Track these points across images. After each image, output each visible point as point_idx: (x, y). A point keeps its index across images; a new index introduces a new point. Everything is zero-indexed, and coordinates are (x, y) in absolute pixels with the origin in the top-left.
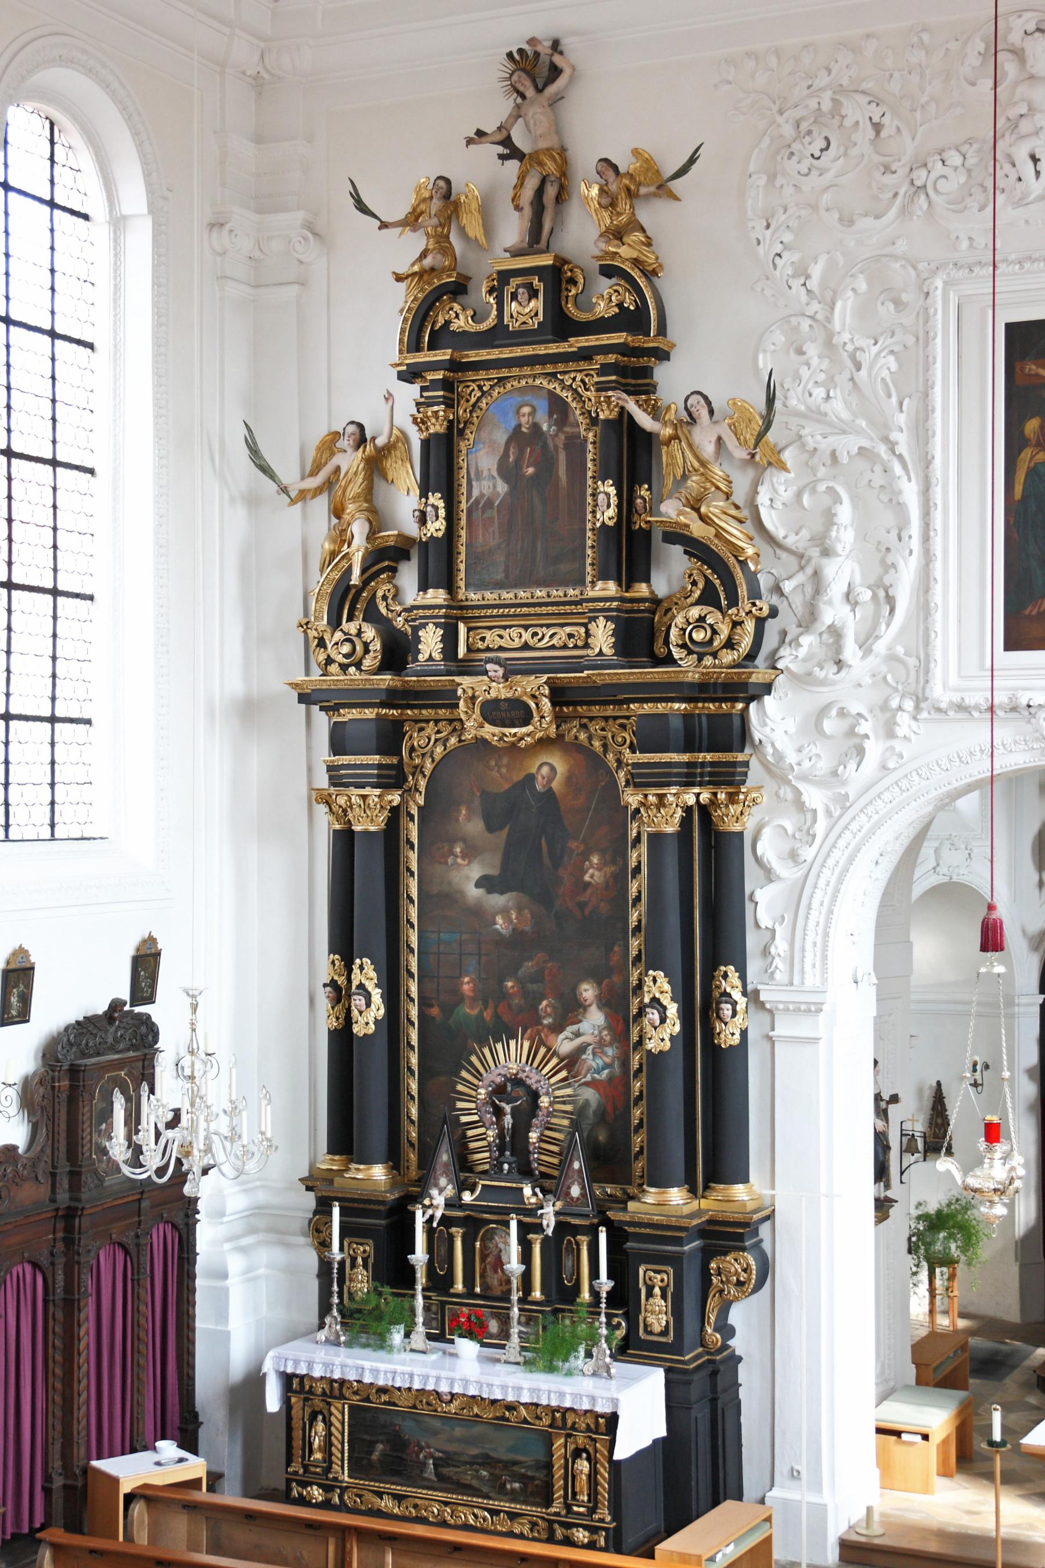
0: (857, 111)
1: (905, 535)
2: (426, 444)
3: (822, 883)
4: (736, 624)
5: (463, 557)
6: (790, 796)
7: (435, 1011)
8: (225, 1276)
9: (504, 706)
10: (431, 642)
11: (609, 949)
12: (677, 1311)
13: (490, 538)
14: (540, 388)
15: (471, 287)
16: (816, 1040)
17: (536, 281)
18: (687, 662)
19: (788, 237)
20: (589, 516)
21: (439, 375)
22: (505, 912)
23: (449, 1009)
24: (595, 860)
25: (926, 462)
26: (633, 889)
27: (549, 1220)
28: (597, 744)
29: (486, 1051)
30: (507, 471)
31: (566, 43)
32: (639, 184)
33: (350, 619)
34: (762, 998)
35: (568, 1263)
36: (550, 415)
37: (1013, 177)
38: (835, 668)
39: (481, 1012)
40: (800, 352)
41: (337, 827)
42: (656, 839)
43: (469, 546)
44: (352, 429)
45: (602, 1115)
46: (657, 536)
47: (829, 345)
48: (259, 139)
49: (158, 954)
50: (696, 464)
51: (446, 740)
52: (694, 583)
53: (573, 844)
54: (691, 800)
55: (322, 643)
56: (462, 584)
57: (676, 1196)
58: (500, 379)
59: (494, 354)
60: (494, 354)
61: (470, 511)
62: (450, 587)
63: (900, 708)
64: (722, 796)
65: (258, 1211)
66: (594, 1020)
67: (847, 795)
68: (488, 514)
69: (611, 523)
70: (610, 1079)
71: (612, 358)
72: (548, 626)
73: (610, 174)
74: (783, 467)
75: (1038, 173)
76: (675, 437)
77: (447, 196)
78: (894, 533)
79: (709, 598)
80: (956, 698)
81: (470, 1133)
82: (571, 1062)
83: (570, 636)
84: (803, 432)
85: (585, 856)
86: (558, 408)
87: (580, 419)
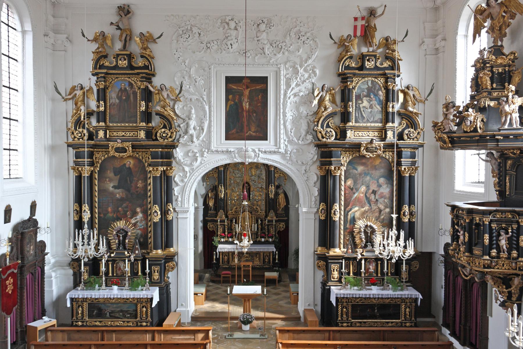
0: (195, 30)
1: (205, 116)
2: (98, 91)
3: (188, 186)
5: (108, 116)
6: (181, 168)
7: (102, 215)
9: (120, 149)
10: (101, 134)
11: (143, 201)
12: (160, 275)
14: (126, 80)
15: (108, 56)
17: (125, 57)
18: (161, 140)
19: (181, 54)
21: (103, 75)
22: (119, 193)
23: (105, 215)
24: (140, 182)
25: (210, 102)
26: (149, 188)
27: (132, 258)
28: (141, 157)
29: (115, 223)
30: (119, 97)
31: (131, 6)
32: (149, 39)
33: (79, 128)
34: (176, 210)
36: (129, 86)
37: (227, 47)
40: (184, 78)
41: (76, 175)
42: (155, 178)
43: (109, 113)
44: (79, 85)
45: (141, 235)
46: (154, 114)
47: (190, 76)
48: (54, 17)
49: (36, 205)
50: (163, 99)
51: (104, 156)
52: (161, 124)
53: (135, 179)
54: (162, 169)
55: (73, 133)
56: (108, 121)
57: (160, 251)
58: (117, 77)
59: (114, 72)
60: (114, 72)
62: (105, 122)
63: (205, 151)
64: (169, 168)
65: (56, 262)
66: (140, 216)
68: (114, 107)
70: (144, 228)
71: (144, 75)
72: (129, 132)
73: (143, 36)
74: (180, 101)
75: (232, 48)
76: (158, 93)
77: (104, 36)
78: (203, 116)
79: (165, 127)
80: (216, 149)
81: (111, 241)
82: (135, 225)
83: (134, 134)
84: (184, 94)
85: (138, 181)
86: (131, 85)
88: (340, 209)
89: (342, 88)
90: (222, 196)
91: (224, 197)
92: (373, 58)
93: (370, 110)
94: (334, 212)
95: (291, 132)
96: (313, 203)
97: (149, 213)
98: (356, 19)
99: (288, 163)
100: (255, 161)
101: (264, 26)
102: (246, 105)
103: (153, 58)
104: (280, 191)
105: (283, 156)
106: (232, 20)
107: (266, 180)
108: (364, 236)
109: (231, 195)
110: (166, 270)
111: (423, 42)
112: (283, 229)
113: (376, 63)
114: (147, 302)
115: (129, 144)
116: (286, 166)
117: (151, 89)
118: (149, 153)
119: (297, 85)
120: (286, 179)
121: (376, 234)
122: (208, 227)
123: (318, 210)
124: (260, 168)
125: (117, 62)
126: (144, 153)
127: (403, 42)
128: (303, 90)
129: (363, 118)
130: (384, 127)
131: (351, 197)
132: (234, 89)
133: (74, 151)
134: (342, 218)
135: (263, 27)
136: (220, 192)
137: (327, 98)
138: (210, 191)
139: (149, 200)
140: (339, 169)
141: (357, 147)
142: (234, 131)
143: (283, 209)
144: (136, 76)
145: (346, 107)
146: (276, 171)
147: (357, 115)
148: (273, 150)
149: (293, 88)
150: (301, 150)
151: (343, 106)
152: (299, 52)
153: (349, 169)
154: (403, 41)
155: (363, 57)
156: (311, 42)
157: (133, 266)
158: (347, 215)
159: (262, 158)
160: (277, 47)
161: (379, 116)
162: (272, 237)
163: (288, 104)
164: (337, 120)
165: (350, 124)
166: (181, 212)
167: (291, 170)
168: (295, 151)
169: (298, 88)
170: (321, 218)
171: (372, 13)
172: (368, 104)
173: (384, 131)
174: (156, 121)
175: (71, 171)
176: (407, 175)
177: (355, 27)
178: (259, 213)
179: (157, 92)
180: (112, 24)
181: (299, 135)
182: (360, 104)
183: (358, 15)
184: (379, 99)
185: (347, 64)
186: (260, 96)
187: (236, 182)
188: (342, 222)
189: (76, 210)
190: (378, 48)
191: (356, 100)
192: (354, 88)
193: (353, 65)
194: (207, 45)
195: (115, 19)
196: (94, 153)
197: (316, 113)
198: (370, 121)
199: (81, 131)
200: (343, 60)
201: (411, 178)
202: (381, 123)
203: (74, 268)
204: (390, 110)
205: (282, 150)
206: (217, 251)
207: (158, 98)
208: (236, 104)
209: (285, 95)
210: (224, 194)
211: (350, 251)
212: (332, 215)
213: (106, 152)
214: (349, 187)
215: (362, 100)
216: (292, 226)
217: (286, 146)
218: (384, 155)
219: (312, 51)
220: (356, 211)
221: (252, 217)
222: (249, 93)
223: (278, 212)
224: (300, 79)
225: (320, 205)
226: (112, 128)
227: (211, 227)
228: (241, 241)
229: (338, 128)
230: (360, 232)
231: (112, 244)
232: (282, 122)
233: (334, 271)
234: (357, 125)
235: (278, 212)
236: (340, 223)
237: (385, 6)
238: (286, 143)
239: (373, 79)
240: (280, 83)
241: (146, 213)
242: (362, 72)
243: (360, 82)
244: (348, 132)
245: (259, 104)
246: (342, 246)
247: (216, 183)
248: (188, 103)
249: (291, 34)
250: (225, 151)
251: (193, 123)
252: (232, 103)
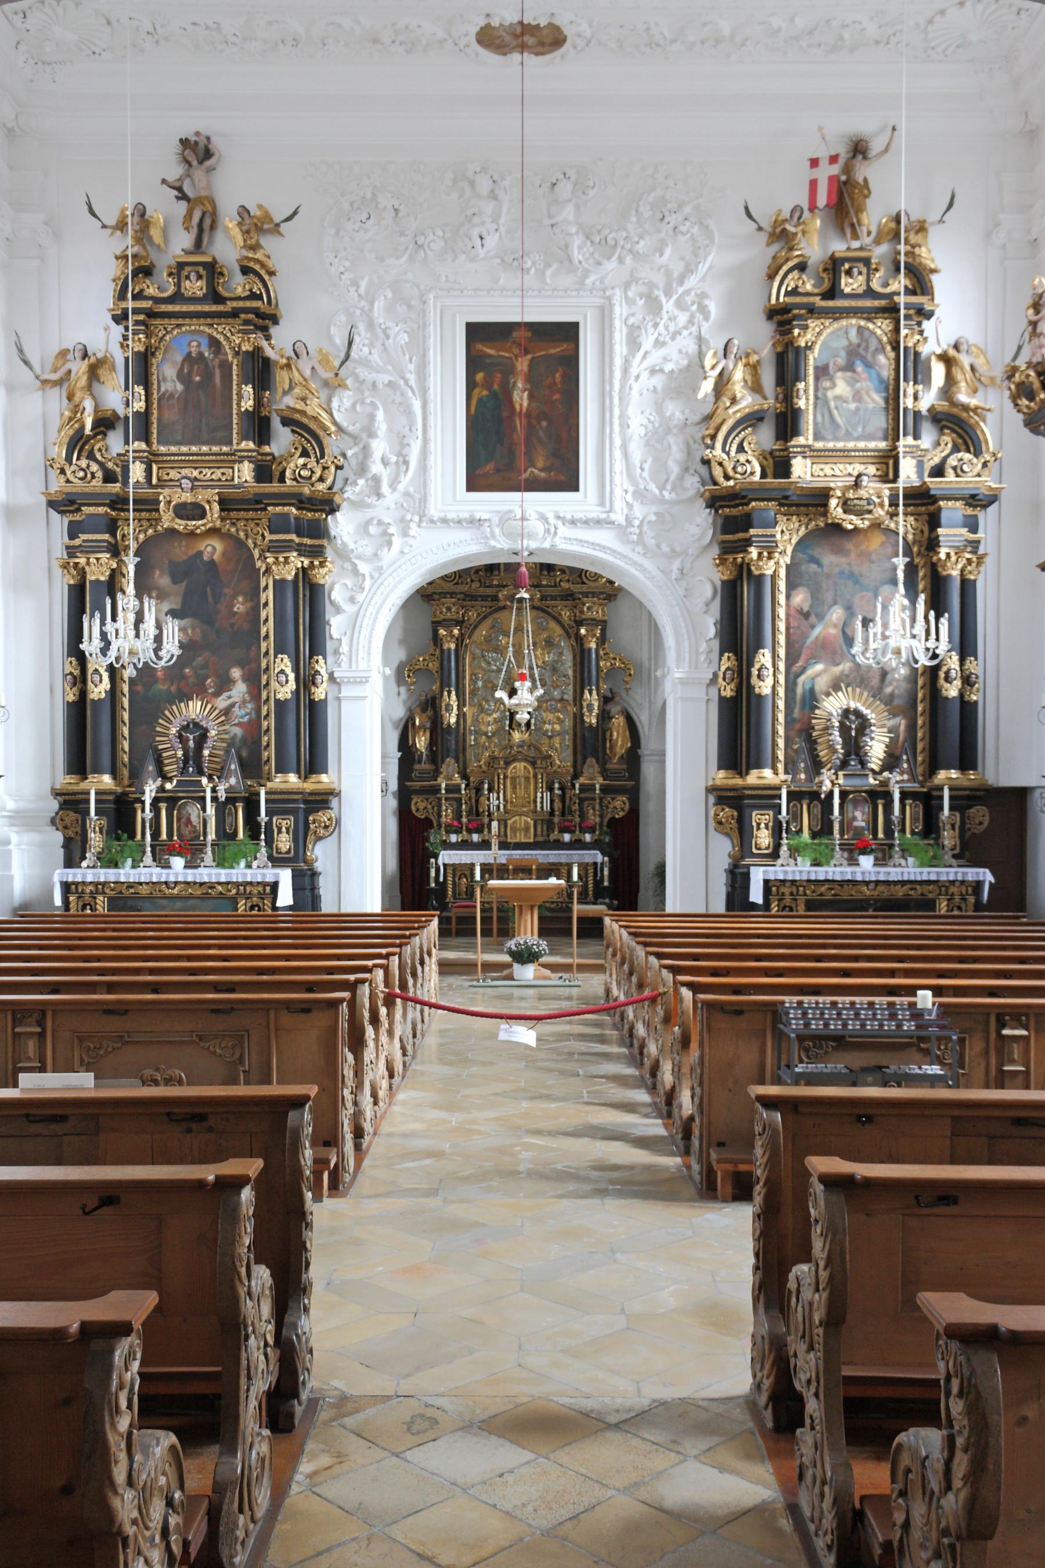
1: (414, 429)
3: (368, 614)
4: (324, 468)
5: (155, 425)
6: (350, 567)
7: (139, 688)
8: (8, 842)
9: (189, 507)
11: (249, 648)
12: (295, 840)
13: (171, 416)
14: (203, 332)
15: (155, 272)
16: (364, 698)
17: (201, 269)
20: (235, 406)
24: (240, 599)
25: (424, 391)
26: (263, 615)
28: (242, 535)
29: (174, 708)
30: (181, 377)
31: (212, 139)
32: (263, 223)
34: (336, 675)
35: (229, 820)
36: (210, 346)
37: (470, 246)
38: (376, 498)
39: (169, 688)
41: (72, 582)
42: (279, 585)
43: (159, 419)
45: (244, 740)
46: (276, 422)
47: (371, 325)
50: (301, 379)
51: (145, 531)
52: (296, 449)
53: (226, 591)
54: (299, 565)
55: (63, 471)
56: (155, 441)
61: (159, 400)
62: (148, 443)
63: (411, 520)
64: (316, 563)
66: (240, 690)
67: (382, 567)
68: (171, 402)
69: (251, 409)
70: (250, 721)
71: (251, 316)
72: (209, 468)
73: (246, 216)
76: (288, 366)
77: (143, 215)
78: (407, 428)
79: (305, 454)
80: (442, 515)
81: (164, 755)
82: (227, 712)
84: (357, 371)
85: (234, 597)
86: (214, 343)
87: (229, 351)
88: (774, 665)
89: (779, 349)
90: (453, 720)
91: (458, 722)
92: (861, 265)
93: (853, 406)
94: (759, 670)
95: (642, 469)
96: (703, 657)
97: (264, 682)
98: (814, 163)
99: (633, 550)
100: (547, 545)
101: (569, 187)
102: (521, 399)
103: (271, 273)
104: (614, 709)
105: (622, 531)
106: (484, 170)
107: (575, 677)
108: (840, 740)
109: (476, 721)
110: (310, 833)
111: (997, 224)
112: (622, 814)
113: (868, 280)
114: (261, 896)
115: (212, 494)
116: (630, 559)
117: (269, 353)
118: (265, 522)
119: (659, 344)
120: (630, 675)
121: (872, 732)
122: (413, 808)
123: (715, 675)
124: (558, 646)
125: (178, 285)
126: (252, 524)
127: (942, 225)
128: (675, 356)
129: (837, 426)
130: (891, 451)
131: (805, 637)
132: (490, 356)
133: (66, 521)
134: (781, 692)
135: (565, 189)
136: (447, 710)
137: (739, 374)
138: (418, 710)
139: (264, 645)
140: (770, 558)
141: (819, 499)
142: (489, 467)
143: (622, 757)
144: (230, 320)
145: (788, 396)
146: (601, 653)
147: (819, 419)
148: (594, 515)
149: (646, 353)
150: (668, 517)
151: (781, 397)
152: (661, 255)
153: (797, 561)
154: (941, 221)
155: (834, 266)
156: (695, 230)
157: (223, 808)
158: (795, 684)
159: (565, 538)
160: (603, 242)
161: (880, 422)
162: (592, 830)
163: (635, 393)
164: (765, 437)
165: (801, 440)
166: (349, 682)
167: (643, 570)
168: (653, 518)
169: (662, 352)
170: (723, 694)
171: (859, 149)
172: (848, 389)
173: (891, 462)
174: (282, 440)
175: (58, 572)
176: (955, 573)
177: (813, 184)
178: (555, 768)
179: (284, 361)
180: (164, 181)
181: (665, 477)
182: (826, 389)
183: (823, 154)
184: (879, 375)
185: (792, 285)
186: (557, 375)
188: (781, 704)
189: (71, 673)
190: (877, 242)
191: (817, 379)
192: (809, 348)
193: (809, 287)
194: (418, 239)
195: (174, 171)
196: (120, 523)
197: (709, 417)
198: (855, 434)
199: (84, 466)
200: (781, 273)
201: (967, 587)
202: (886, 439)
203: (66, 827)
204: (909, 402)
205: (618, 517)
206: (440, 862)
207: (287, 381)
208: (494, 395)
209: (626, 370)
210: (458, 715)
211: (803, 776)
212: (754, 680)
213: (149, 520)
214: (800, 612)
215: (831, 379)
216: (648, 808)
217: (630, 506)
218: (892, 526)
219: (697, 252)
220: (818, 675)
221: (535, 776)
222: (530, 366)
223: (609, 766)
224: (666, 328)
225: (720, 660)
226: (165, 458)
227: (421, 808)
228: (513, 692)
229: (768, 457)
230: (827, 729)
231: (166, 762)
232: (618, 442)
233: (758, 828)
234: (819, 445)
235: (609, 766)
236: (775, 706)
237: (894, 129)
238: (629, 498)
239: (862, 323)
240: (611, 337)
241: (255, 682)
242: (831, 303)
243: (828, 331)
244: (794, 462)
245: (557, 396)
246: (780, 767)
247: (435, 687)
248: (367, 393)
249: (641, 209)
250: (465, 520)
251: (379, 447)
252: (485, 393)
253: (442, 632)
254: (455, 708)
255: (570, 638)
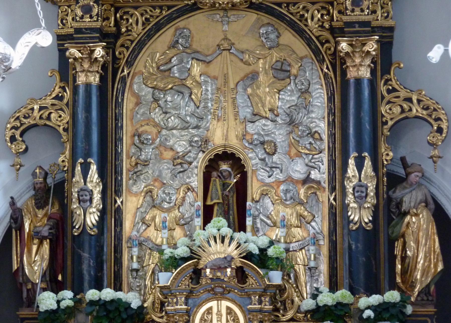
107: (332, 136)
120: (440, 130)
143: (425, 291)
146: (383, 89)
187: (168, 155)
210: (103, 213)
253: (74, 52)
254: (97, 197)
255: (321, 61)
